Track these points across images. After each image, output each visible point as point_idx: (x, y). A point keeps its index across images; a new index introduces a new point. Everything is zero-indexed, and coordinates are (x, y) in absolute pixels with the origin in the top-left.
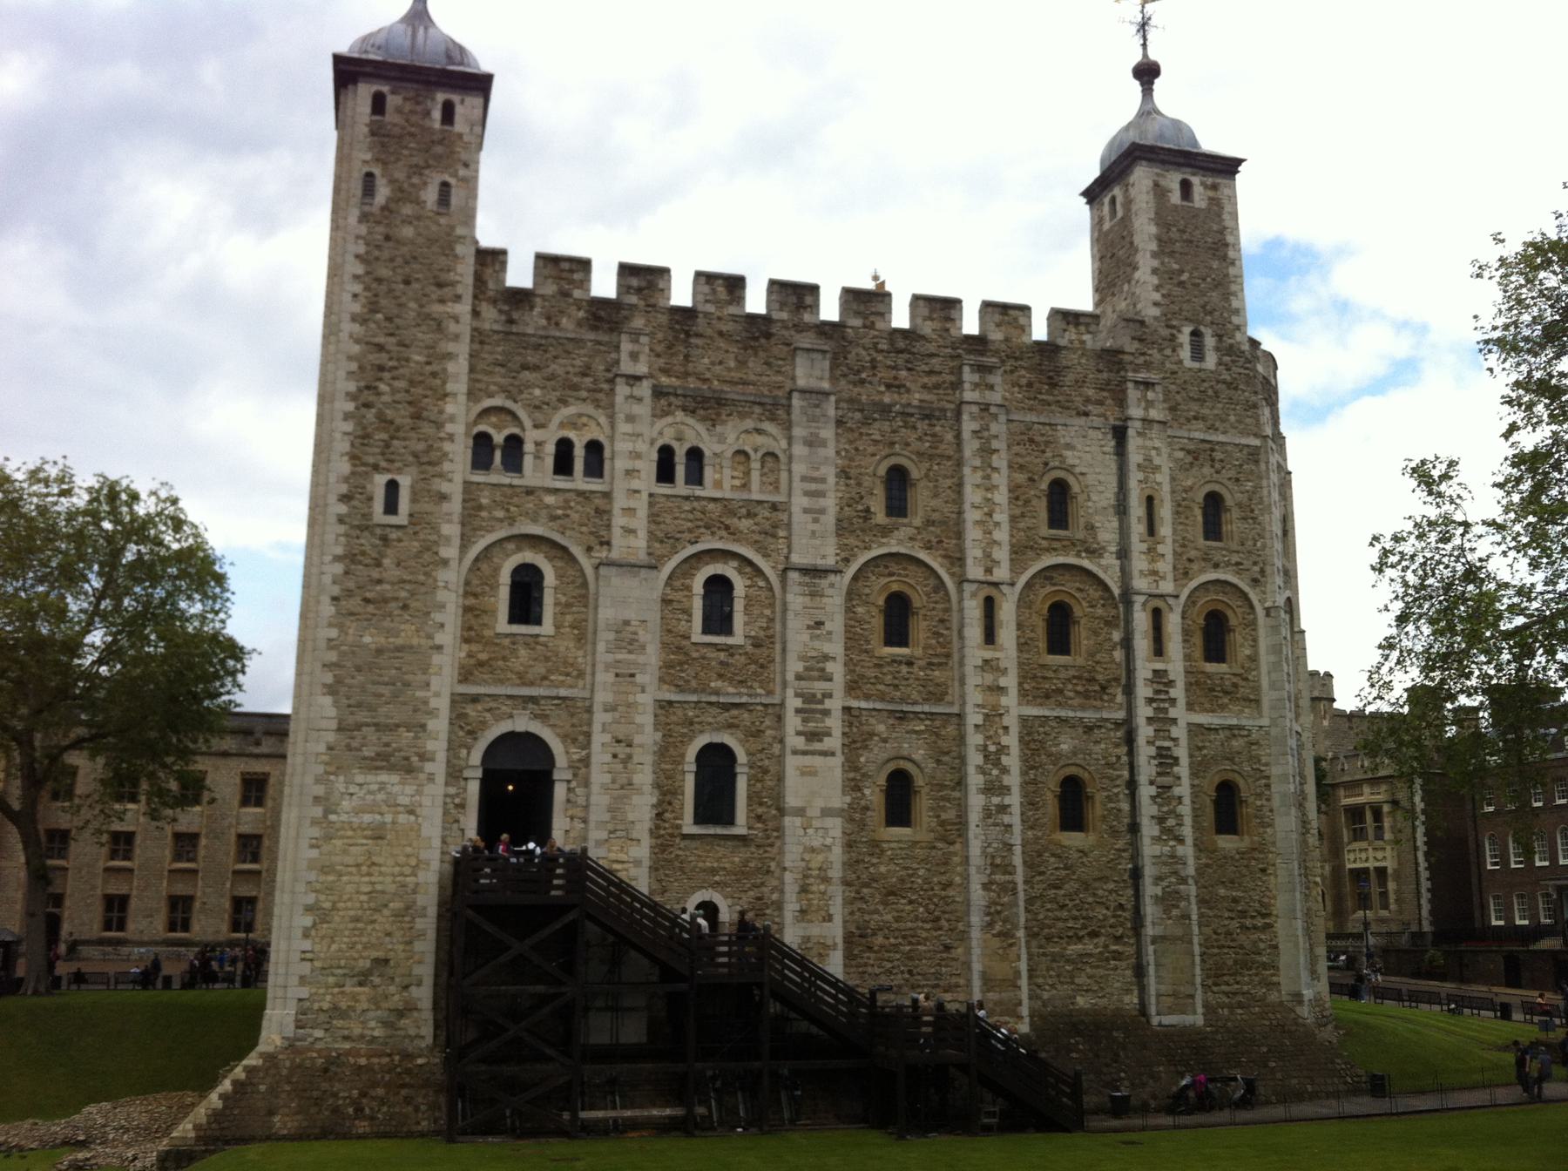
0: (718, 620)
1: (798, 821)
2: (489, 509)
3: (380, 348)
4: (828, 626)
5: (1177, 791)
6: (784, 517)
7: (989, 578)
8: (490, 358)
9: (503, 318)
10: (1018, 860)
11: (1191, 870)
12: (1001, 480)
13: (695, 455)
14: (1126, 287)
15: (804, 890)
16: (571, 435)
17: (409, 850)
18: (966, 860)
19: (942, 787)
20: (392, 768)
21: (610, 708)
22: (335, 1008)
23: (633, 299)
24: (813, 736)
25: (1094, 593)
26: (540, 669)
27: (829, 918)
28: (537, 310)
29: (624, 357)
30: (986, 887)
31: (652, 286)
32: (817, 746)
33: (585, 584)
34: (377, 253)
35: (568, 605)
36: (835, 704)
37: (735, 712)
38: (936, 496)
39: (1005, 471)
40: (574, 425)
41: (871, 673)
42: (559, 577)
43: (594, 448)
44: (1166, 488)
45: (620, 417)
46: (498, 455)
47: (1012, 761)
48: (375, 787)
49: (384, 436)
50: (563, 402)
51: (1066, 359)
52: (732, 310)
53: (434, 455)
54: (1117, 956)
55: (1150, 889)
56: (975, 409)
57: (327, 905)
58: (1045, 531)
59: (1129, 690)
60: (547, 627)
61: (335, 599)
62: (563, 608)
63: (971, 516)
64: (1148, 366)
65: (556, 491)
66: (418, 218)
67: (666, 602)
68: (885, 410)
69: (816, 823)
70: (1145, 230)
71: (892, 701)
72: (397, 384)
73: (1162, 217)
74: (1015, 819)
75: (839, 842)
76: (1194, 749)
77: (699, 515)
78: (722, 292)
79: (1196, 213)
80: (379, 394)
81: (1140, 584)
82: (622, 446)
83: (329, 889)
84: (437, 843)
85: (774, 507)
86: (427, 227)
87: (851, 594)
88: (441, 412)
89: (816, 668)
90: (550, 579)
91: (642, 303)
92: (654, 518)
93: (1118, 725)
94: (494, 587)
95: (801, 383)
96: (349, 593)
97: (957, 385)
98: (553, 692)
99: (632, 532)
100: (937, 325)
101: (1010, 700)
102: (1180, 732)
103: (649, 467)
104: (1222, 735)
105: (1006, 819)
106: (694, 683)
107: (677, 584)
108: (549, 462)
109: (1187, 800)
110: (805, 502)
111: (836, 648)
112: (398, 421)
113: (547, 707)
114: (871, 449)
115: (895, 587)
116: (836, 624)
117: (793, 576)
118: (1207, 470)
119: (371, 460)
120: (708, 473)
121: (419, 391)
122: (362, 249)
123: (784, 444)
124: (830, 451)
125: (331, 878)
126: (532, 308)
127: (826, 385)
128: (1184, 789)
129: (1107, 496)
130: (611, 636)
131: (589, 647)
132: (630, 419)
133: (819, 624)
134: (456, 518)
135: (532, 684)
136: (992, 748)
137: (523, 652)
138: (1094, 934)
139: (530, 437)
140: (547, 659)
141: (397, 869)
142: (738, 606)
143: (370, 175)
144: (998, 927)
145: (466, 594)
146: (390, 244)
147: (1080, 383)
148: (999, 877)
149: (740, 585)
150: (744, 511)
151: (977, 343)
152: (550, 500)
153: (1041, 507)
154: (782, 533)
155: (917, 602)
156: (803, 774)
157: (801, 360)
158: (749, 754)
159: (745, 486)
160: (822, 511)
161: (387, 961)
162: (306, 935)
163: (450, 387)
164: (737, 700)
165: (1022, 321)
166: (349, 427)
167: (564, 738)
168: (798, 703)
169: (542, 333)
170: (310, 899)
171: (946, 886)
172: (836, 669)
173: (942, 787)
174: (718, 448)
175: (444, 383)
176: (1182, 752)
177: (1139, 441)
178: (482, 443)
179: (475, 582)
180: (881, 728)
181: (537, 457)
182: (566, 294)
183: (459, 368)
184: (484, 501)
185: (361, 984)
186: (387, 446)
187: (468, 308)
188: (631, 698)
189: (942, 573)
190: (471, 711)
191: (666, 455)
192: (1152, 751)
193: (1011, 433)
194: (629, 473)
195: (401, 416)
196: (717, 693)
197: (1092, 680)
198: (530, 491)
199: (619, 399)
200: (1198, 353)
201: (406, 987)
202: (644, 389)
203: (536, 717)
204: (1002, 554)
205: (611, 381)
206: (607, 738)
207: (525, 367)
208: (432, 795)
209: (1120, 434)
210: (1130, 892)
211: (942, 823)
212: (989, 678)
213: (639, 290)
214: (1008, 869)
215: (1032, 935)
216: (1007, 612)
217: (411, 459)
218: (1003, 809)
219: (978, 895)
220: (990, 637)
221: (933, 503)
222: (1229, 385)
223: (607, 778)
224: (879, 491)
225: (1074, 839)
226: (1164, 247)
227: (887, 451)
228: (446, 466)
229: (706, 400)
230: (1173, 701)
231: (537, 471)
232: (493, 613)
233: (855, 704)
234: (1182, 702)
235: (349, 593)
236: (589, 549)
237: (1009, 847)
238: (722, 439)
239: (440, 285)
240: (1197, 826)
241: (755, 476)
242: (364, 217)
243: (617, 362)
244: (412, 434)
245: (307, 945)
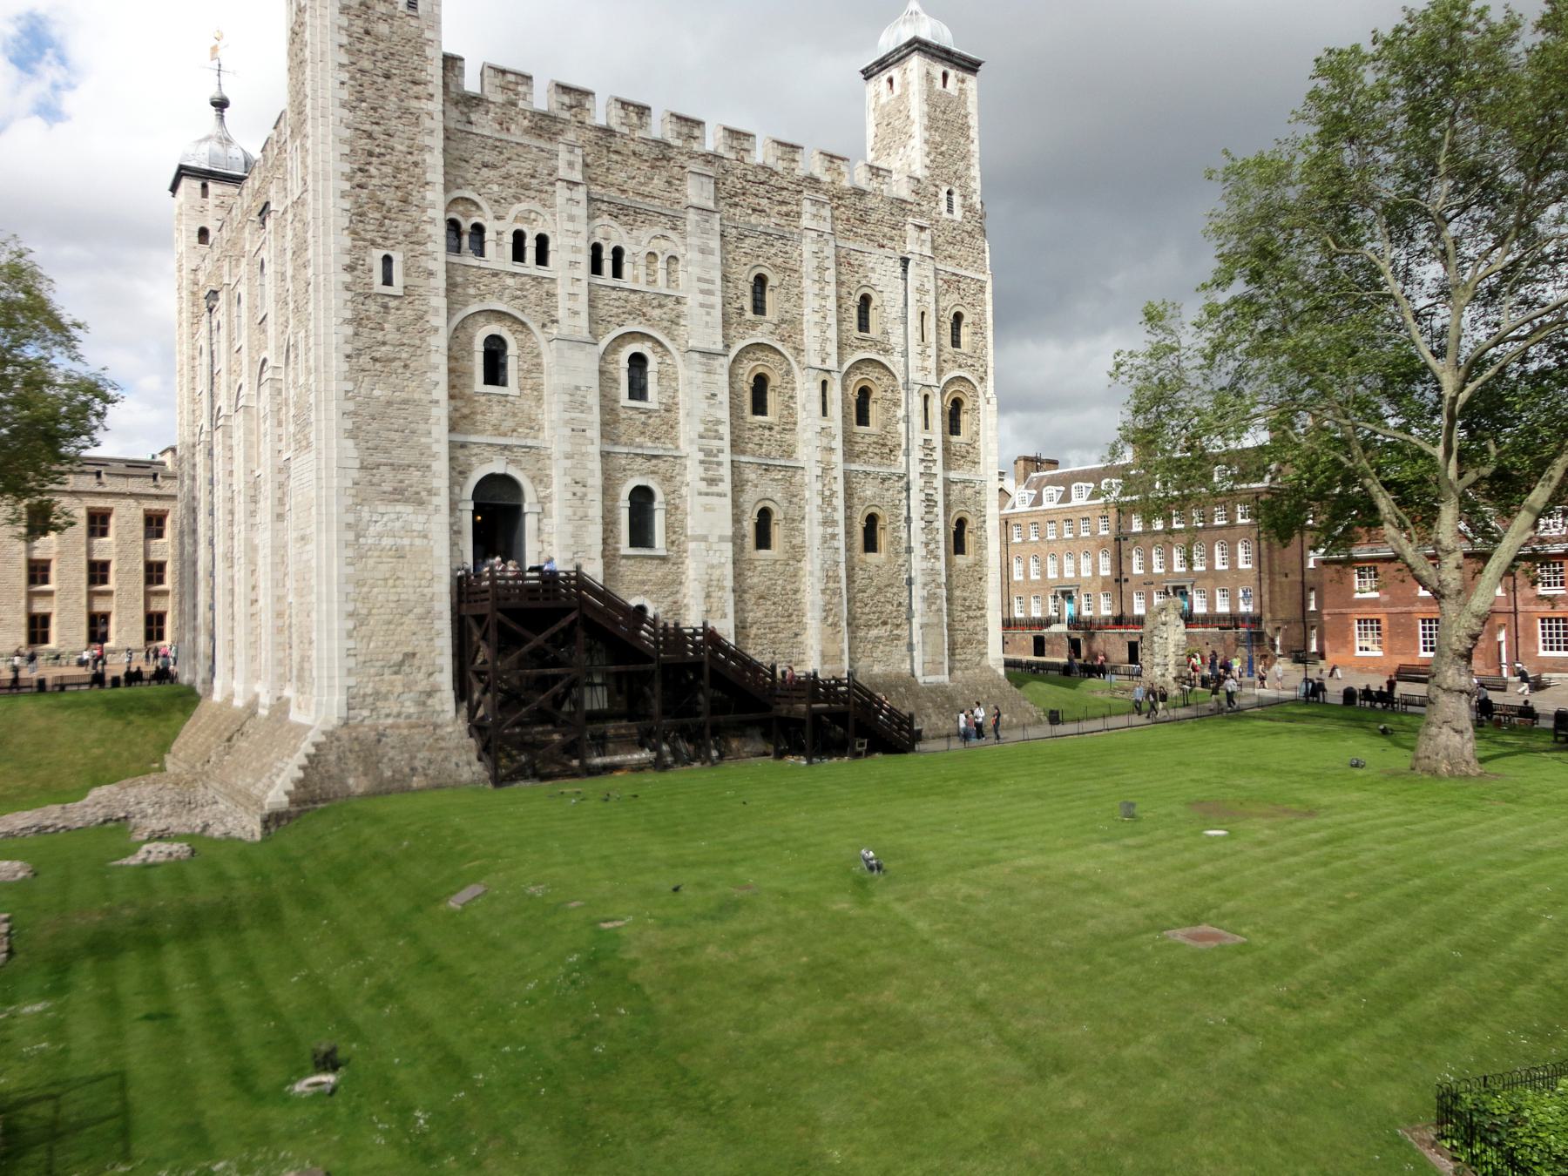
0: (638, 390)
1: (703, 545)
2: (465, 287)
3: (370, 136)
4: (720, 397)
5: (936, 524)
6: (684, 308)
7: (826, 367)
8: (457, 153)
9: (464, 119)
10: (842, 573)
11: (944, 579)
12: (831, 290)
13: (618, 253)
14: (901, 150)
15: (708, 596)
16: (524, 227)
17: (424, 567)
18: (811, 573)
19: (794, 520)
20: (407, 501)
21: (569, 456)
22: (377, 693)
23: (566, 115)
24: (712, 481)
25: (886, 380)
26: (509, 423)
27: (724, 616)
28: (491, 115)
29: (561, 163)
30: (823, 592)
31: (580, 105)
32: (714, 489)
33: (538, 355)
34: (358, 46)
35: (530, 371)
36: (726, 457)
37: (654, 462)
38: (788, 301)
39: (833, 286)
40: (526, 220)
41: (747, 434)
42: (521, 347)
43: (542, 241)
44: (933, 306)
46: (466, 239)
47: (839, 502)
48: (393, 516)
49: (377, 215)
50: (519, 200)
51: (871, 202)
52: (639, 134)
53: (419, 237)
54: (898, 638)
55: (918, 591)
56: (814, 234)
57: (364, 611)
58: (857, 333)
59: (907, 454)
60: (512, 387)
62: (526, 374)
63: (809, 318)
64: (922, 214)
65: (514, 275)
66: (392, 17)
67: (602, 372)
68: (753, 228)
69: (715, 547)
70: (917, 108)
71: (760, 456)
72: (384, 168)
73: (931, 100)
74: (841, 543)
75: (730, 561)
76: (947, 495)
77: (621, 303)
78: (634, 118)
79: (950, 100)
81: (915, 376)
83: (365, 599)
84: (446, 561)
85: (678, 301)
86: (401, 27)
87: (732, 374)
88: (423, 198)
89: (710, 431)
90: (512, 349)
92: (592, 304)
93: (901, 478)
94: (471, 353)
95: (695, 201)
96: (359, 353)
97: (799, 214)
98: (523, 443)
99: (576, 313)
100: (785, 164)
101: (838, 457)
102: (938, 483)
103: (585, 259)
104: (960, 486)
105: (836, 544)
106: (624, 439)
107: (609, 358)
109: (942, 531)
110: (701, 298)
111: (724, 414)
112: (388, 202)
113: (519, 453)
114: (744, 260)
115: (760, 370)
116: (724, 396)
117: (696, 356)
118: (956, 296)
120: (627, 269)
121: (403, 176)
122: (345, 40)
123: (682, 250)
124: (716, 259)
125: (365, 589)
126: (487, 113)
127: (711, 205)
128: (940, 524)
129: (895, 311)
130: (567, 398)
131: (545, 406)
132: (571, 218)
133: (714, 395)
134: (442, 292)
135: (505, 435)
136: (827, 493)
137: (496, 408)
138: (885, 623)
140: (515, 415)
141: (416, 583)
142: (652, 378)
144: (830, 620)
145: (449, 358)
146: (367, 38)
147: (880, 222)
148: (831, 585)
149: (652, 366)
150: (655, 303)
151: (814, 181)
152: (510, 281)
153: (854, 312)
154: (682, 322)
155: (775, 380)
156: (706, 510)
158: (666, 494)
160: (712, 307)
161: (414, 655)
162: (350, 636)
163: (429, 177)
164: (655, 453)
165: (843, 168)
166: (347, 204)
167: (533, 479)
168: (701, 456)
169: (497, 135)
170: (350, 607)
171: (796, 592)
172: (725, 430)
173: (794, 520)
174: (636, 249)
175: (424, 173)
176: (939, 498)
177: (918, 270)
178: (453, 226)
179: (455, 348)
180: (753, 476)
182: (514, 104)
184: (459, 280)
185: (396, 673)
186: (382, 225)
187: (440, 107)
188: (584, 449)
189: (791, 359)
190: (459, 453)
191: (596, 250)
192: (923, 497)
193: (837, 256)
194: (573, 264)
195: (390, 198)
196: (641, 446)
197: (884, 445)
198: (495, 275)
200: (950, 210)
201: (430, 675)
202: (580, 193)
203: (513, 461)
204: (832, 348)
205: (552, 184)
206: (568, 480)
207: (485, 166)
208: (439, 525)
209: (905, 261)
210: (906, 593)
211: (793, 547)
212: (825, 442)
213: (571, 107)
214: (836, 579)
215: (849, 624)
216: (835, 392)
217: (401, 238)
218: (833, 536)
219: (819, 600)
220: (824, 413)
221: (787, 305)
222: (969, 233)
223: (569, 512)
224: (749, 293)
225: (871, 557)
226: (932, 124)
227: (755, 262)
228: (430, 247)
229: (623, 208)
230: (934, 461)
231: (497, 254)
232: (471, 375)
233: (736, 458)
234: (940, 463)
235: (359, 353)
236: (544, 326)
237: (837, 563)
238: (638, 243)
239: (415, 83)
240: (946, 550)
241: (661, 276)
243: (555, 169)
244: (401, 216)
245: (351, 644)
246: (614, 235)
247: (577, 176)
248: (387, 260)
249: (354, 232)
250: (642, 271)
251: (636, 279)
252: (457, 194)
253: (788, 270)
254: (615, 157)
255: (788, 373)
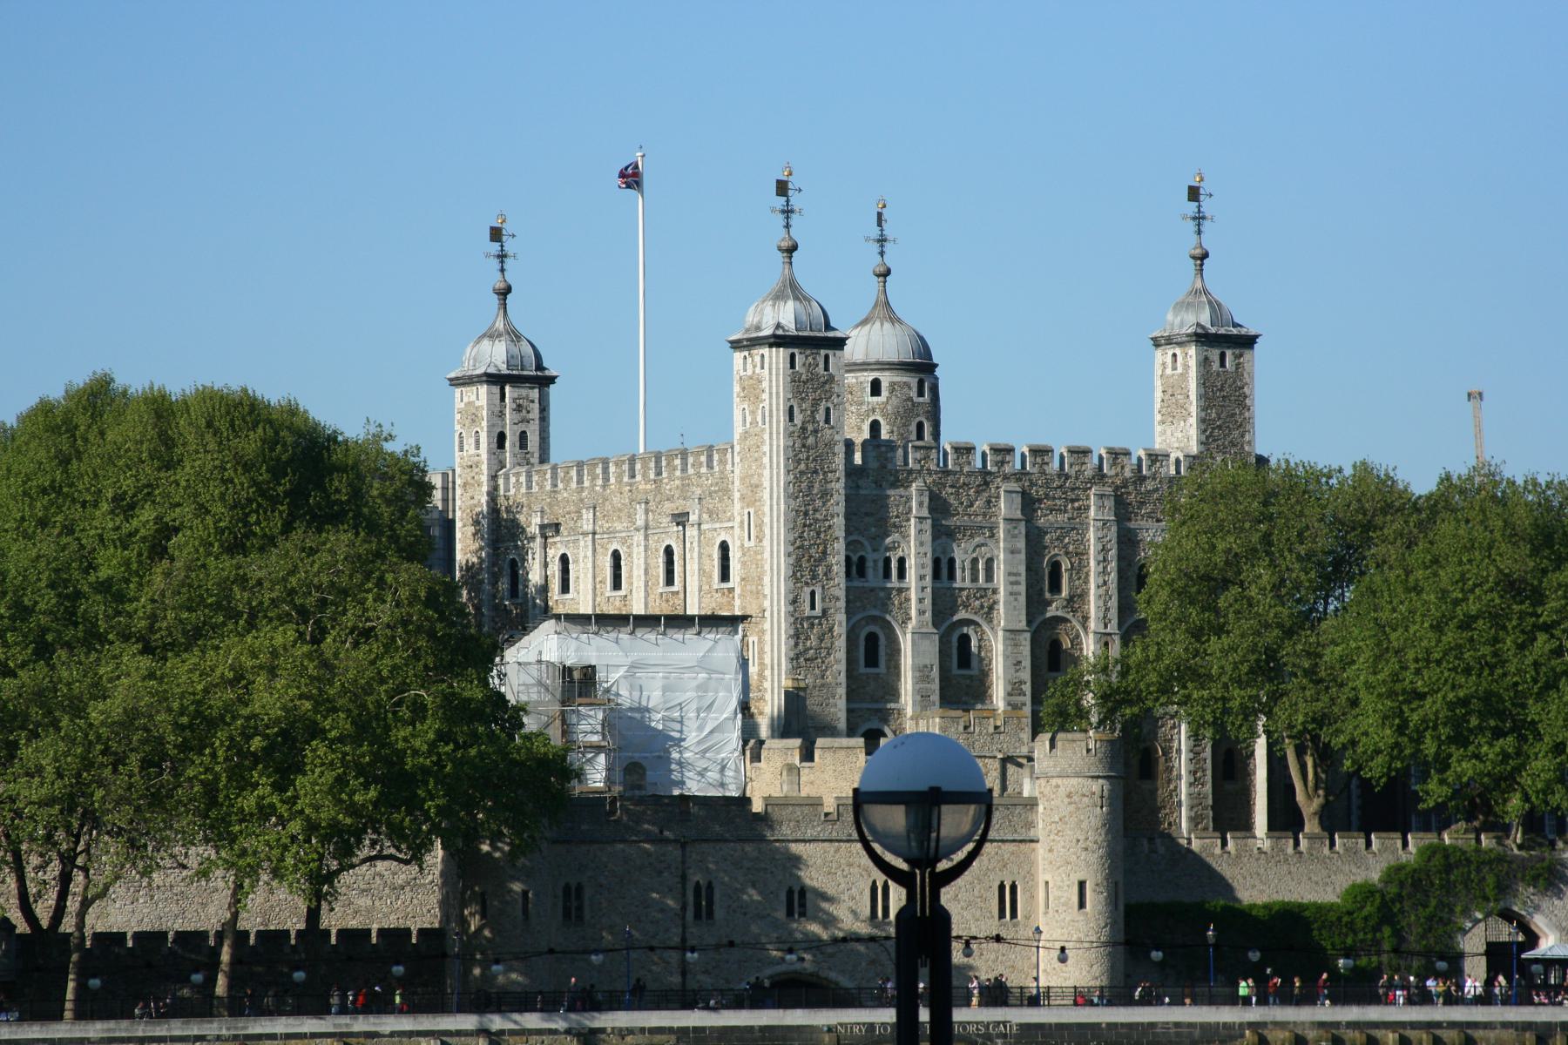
7: (1108, 630)
43: (902, 561)
51: (1150, 485)
62: (888, 661)
108: (881, 571)
116: (1027, 663)
124: (1023, 556)
139: (871, 557)
159: (975, 579)
172: (1027, 688)
181: (875, 569)
198: (872, 590)
207: (867, 514)
247: (925, 513)
250: (967, 573)
251: (963, 580)
252: (851, 538)
253: (1082, 554)
255: (1078, 636)
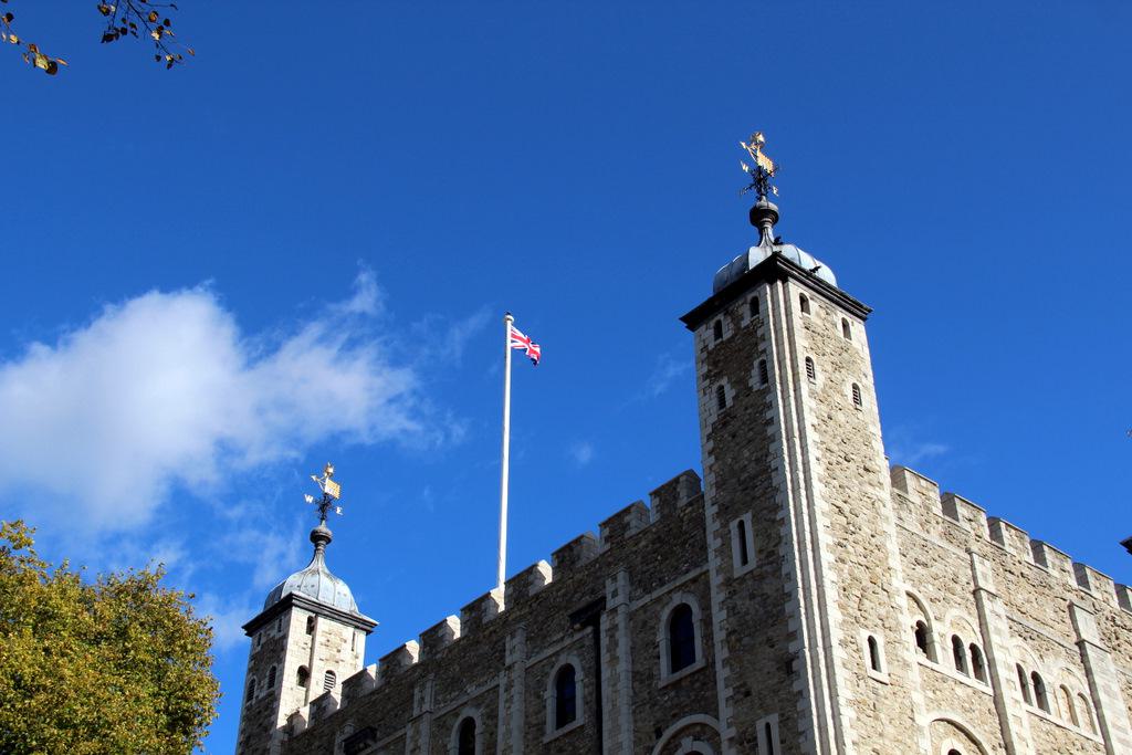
23: (967, 526)
45: (991, 627)
61: (854, 743)
80: (848, 553)
82: (998, 654)
91: (972, 532)
119: (851, 611)
122: (816, 422)
132: (998, 632)
143: (808, 360)
152: (959, 690)
157: (1079, 613)
163: (892, 563)
175: (887, 559)
183: (893, 546)
199: (987, 612)
239: (866, 469)
242: (812, 394)
243: (975, 578)
244: (873, 597)
246: (1029, 659)
248: (872, 642)
249: (841, 606)
254: (1008, 575)
